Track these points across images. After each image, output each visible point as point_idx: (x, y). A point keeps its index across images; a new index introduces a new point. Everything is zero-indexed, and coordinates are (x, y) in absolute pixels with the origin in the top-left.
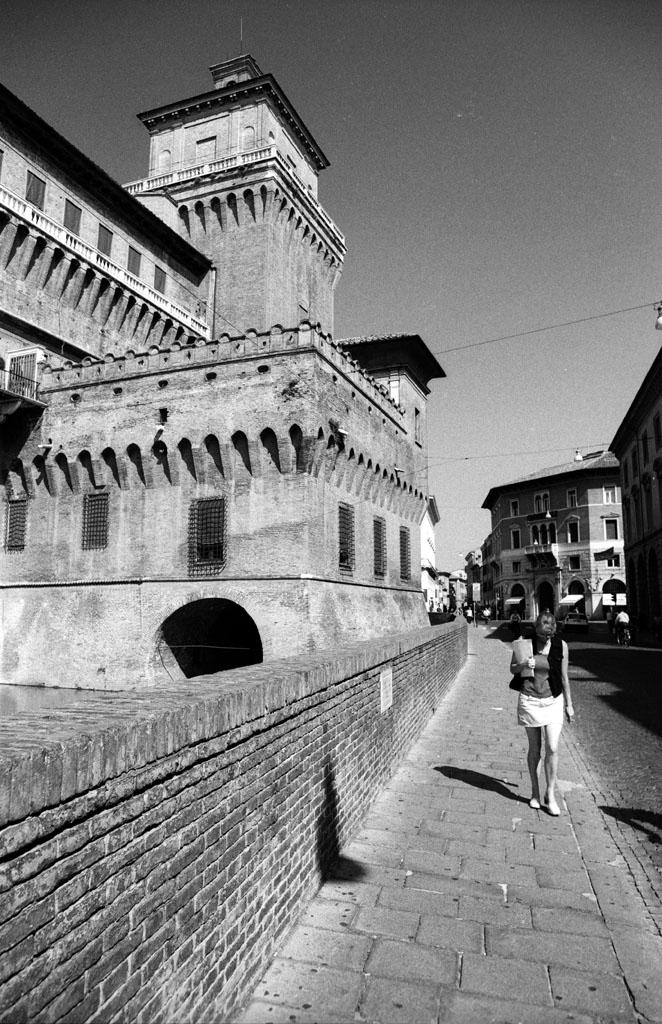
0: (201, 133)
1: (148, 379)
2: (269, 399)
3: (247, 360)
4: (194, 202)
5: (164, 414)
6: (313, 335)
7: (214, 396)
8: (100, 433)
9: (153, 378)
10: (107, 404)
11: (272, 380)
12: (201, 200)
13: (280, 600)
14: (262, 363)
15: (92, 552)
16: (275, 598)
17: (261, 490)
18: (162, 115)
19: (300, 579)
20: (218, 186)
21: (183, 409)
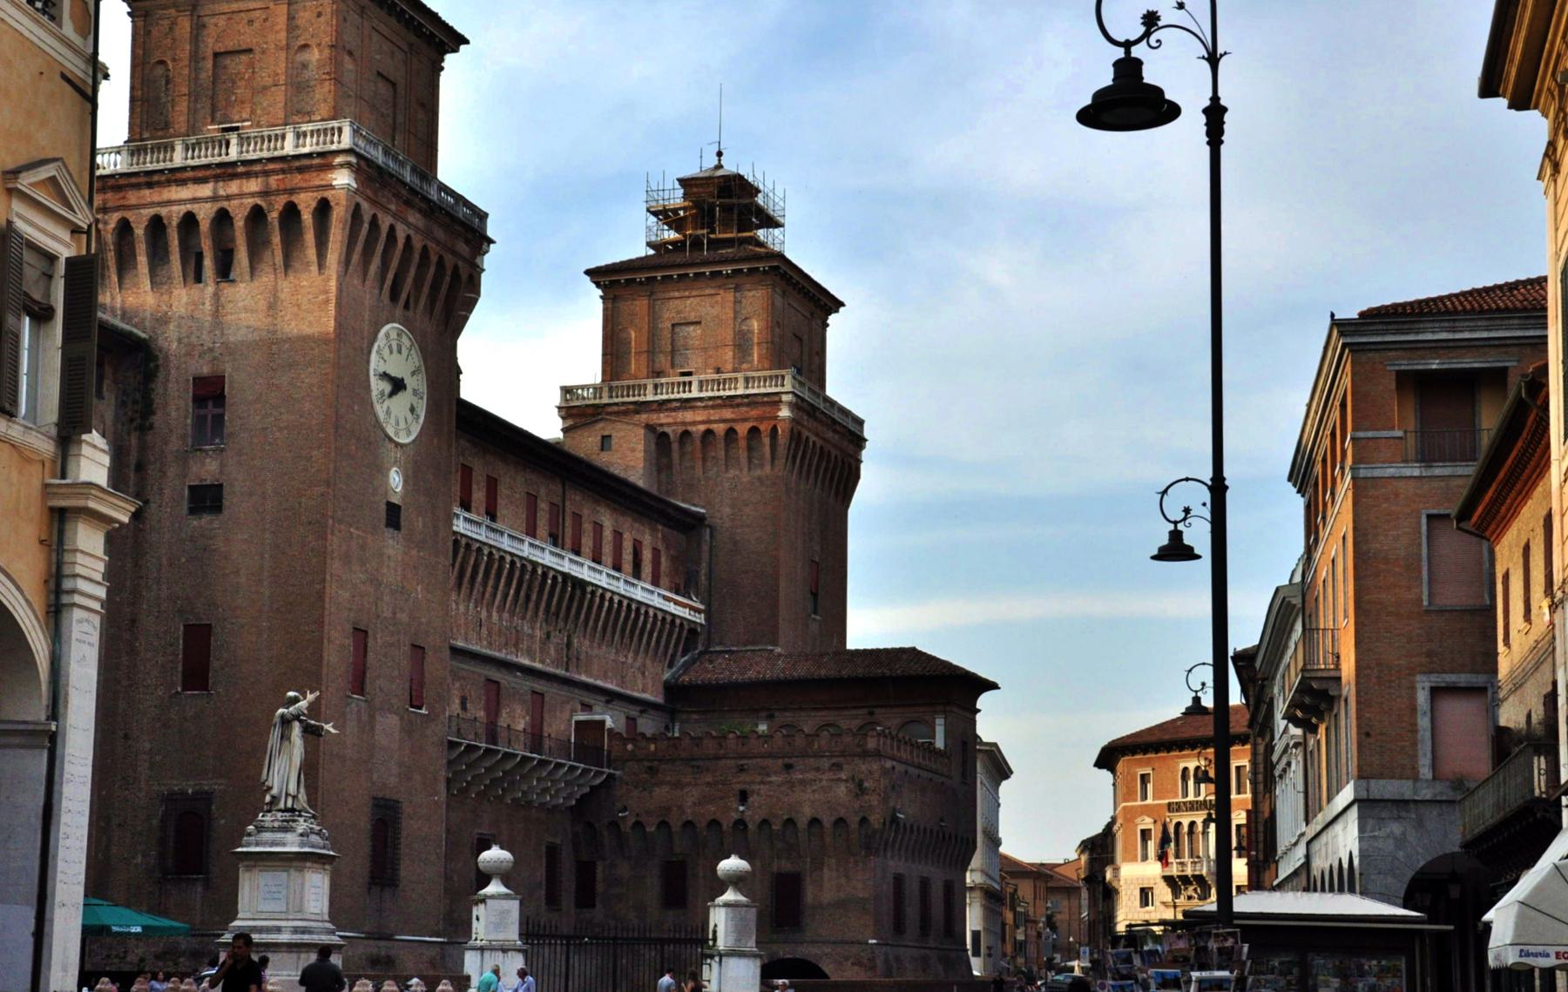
0: (679, 312)
1: (728, 761)
2: (841, 790)
3: (823, 757)
4: (680, 429)
5: (744, 797)
6: (879, 741)
7: (791, 785)
8: (680, 807)
9: (733, 762)
10: (688, 779)
11: (844, 777)
12: (689, 428)
13: (851, 960)
14: (834, 760)
15: (671, 913)
16: (847, 959)
17: (834, 867)
18: (622, 278)
19: (867, 944)
20: (715, 415)
21: (762, 792)
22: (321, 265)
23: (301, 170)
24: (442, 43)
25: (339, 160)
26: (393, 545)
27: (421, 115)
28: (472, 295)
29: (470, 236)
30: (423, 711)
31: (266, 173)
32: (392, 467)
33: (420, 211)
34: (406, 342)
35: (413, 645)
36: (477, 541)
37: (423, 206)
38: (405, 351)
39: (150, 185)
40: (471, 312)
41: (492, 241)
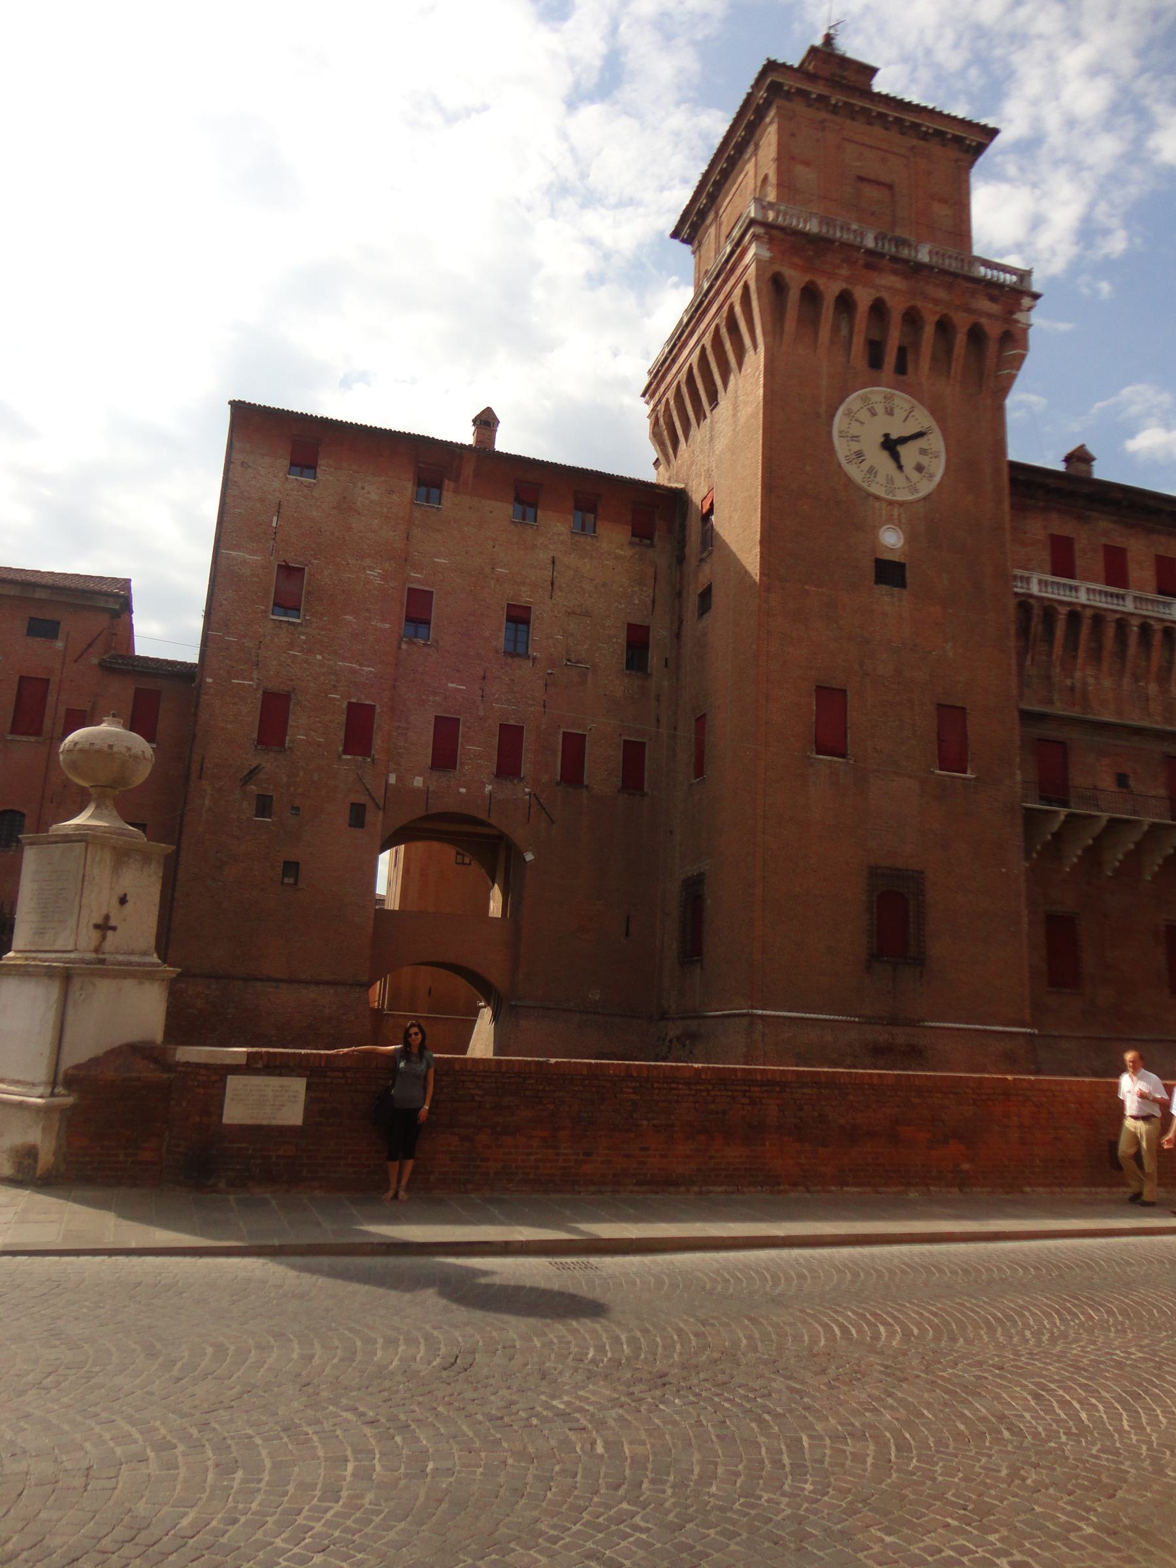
22: (755, 347)
23: (733, 270)
24: (957, 140)
25: (748, 237)
26: (887, 600)
27: (942, 212)
28: (1015, 352)
29: (996, 292)
30: (968, 775)
31: (718, 293)
32: (886, 522)
33: (895, 272)
34: (902, 401)
35: (938, 705)
36: (1116, 611)
37: (899, 266)
38: (900, 414)
39: (674, 361)
40: (1018, 368)
41: (1036, 296)
